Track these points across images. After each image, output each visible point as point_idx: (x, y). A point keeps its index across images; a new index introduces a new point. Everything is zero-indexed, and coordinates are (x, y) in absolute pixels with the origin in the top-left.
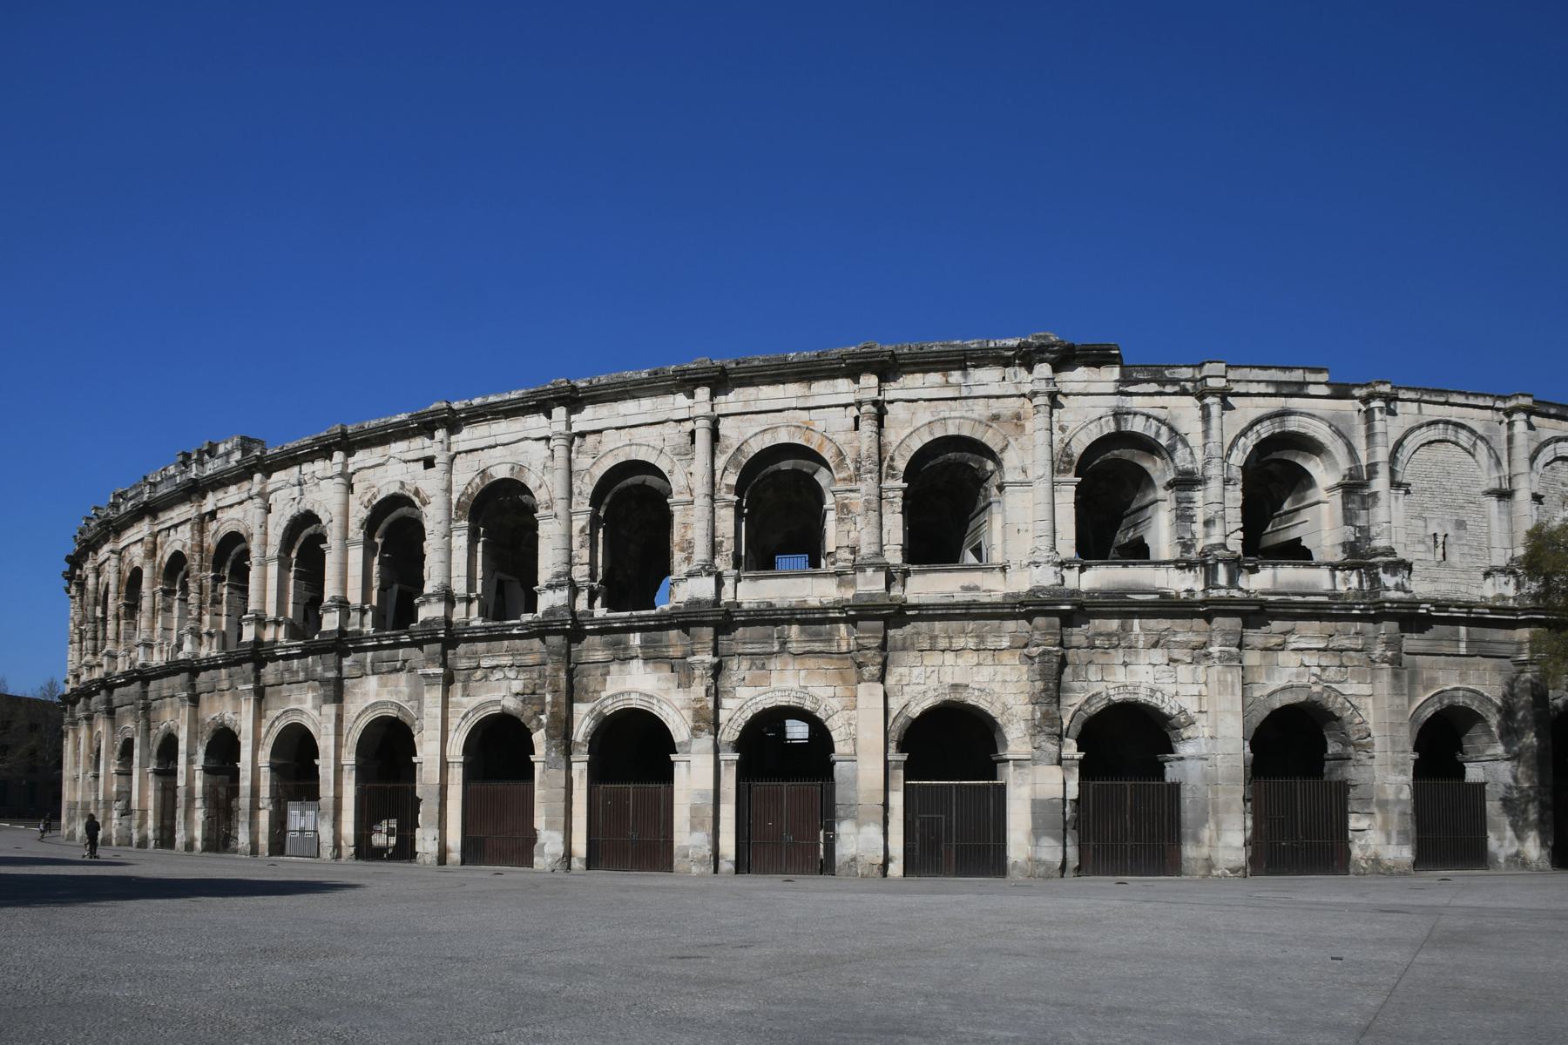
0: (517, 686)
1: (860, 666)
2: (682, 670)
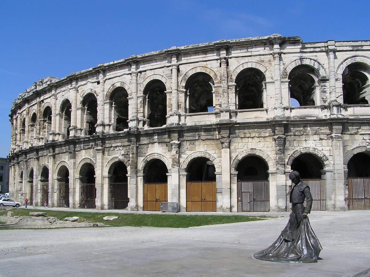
0: (123, 152)
1: (222, 143)
2: (169, 146)
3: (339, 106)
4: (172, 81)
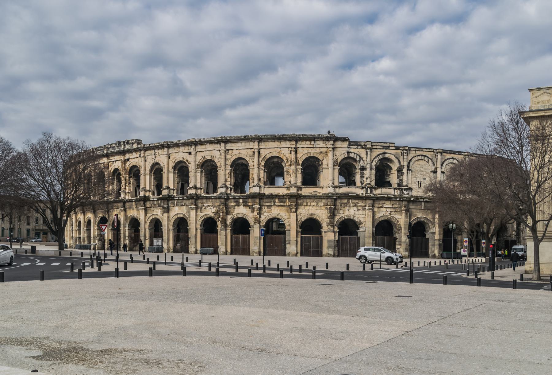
0: (213, 211)
1: (291, 209)
3: (371, 188)
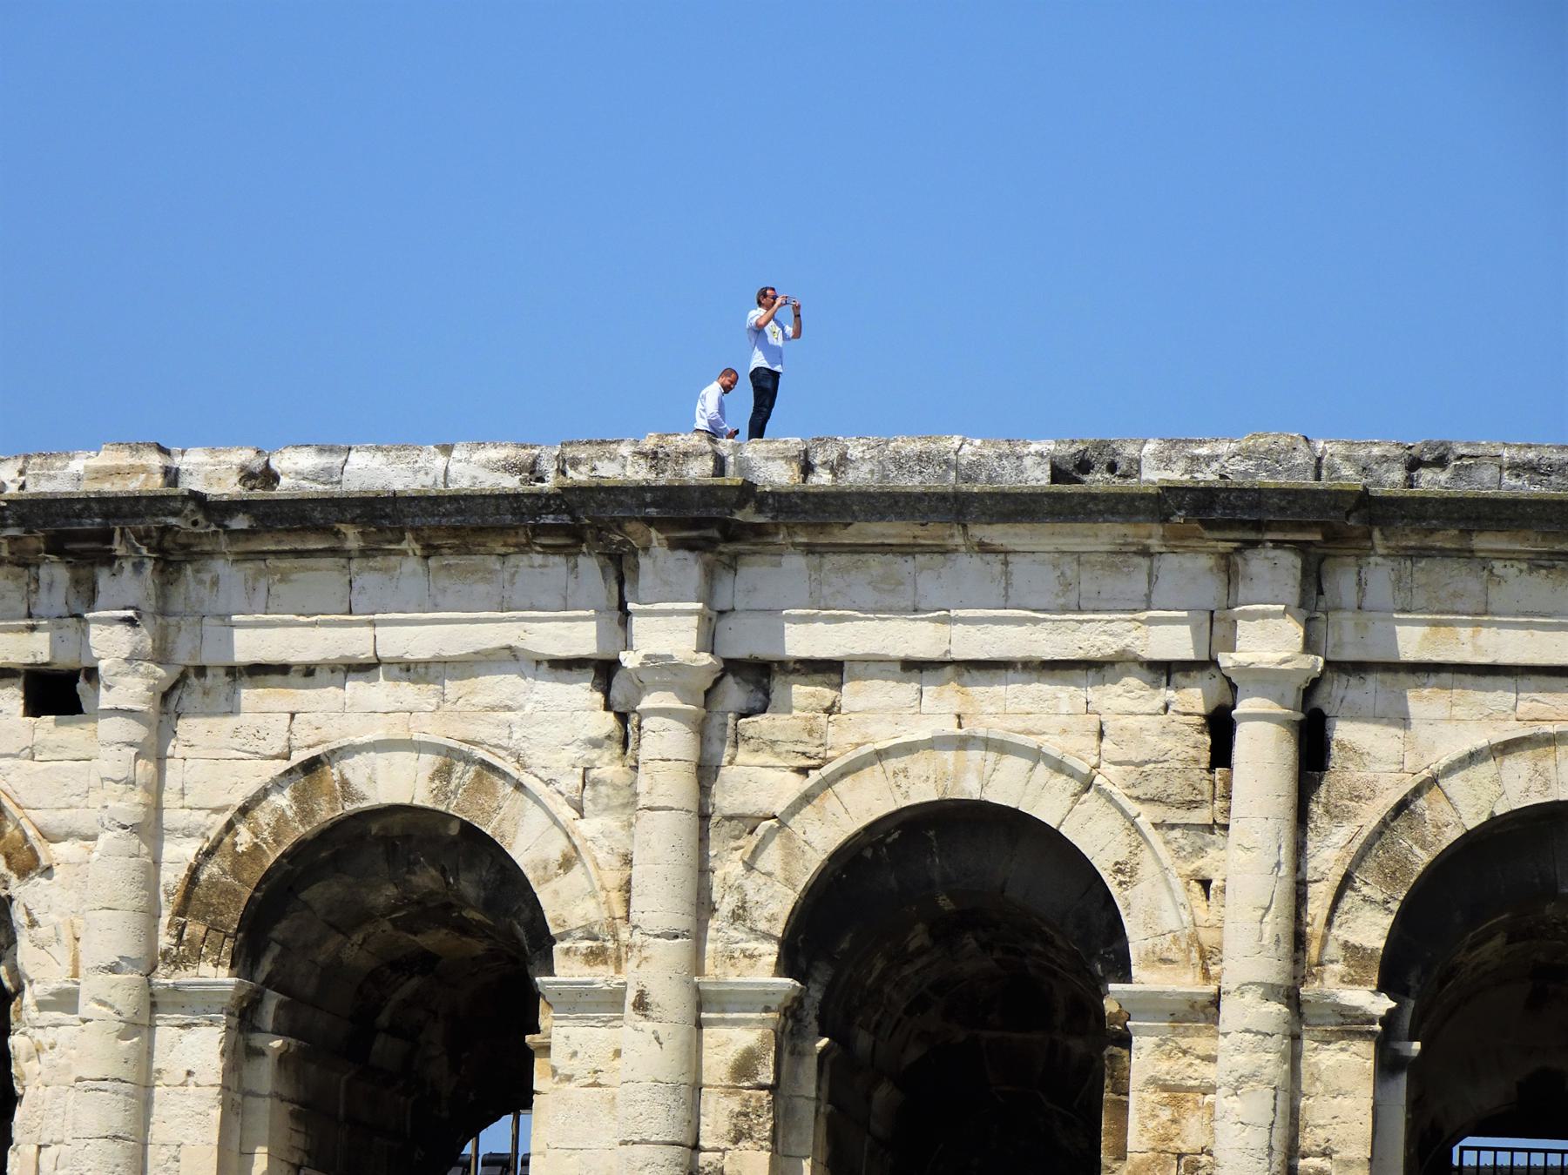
4: (1208, 864)
